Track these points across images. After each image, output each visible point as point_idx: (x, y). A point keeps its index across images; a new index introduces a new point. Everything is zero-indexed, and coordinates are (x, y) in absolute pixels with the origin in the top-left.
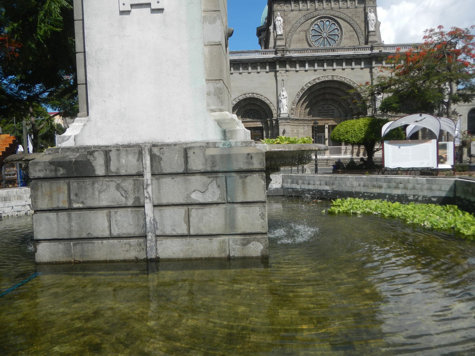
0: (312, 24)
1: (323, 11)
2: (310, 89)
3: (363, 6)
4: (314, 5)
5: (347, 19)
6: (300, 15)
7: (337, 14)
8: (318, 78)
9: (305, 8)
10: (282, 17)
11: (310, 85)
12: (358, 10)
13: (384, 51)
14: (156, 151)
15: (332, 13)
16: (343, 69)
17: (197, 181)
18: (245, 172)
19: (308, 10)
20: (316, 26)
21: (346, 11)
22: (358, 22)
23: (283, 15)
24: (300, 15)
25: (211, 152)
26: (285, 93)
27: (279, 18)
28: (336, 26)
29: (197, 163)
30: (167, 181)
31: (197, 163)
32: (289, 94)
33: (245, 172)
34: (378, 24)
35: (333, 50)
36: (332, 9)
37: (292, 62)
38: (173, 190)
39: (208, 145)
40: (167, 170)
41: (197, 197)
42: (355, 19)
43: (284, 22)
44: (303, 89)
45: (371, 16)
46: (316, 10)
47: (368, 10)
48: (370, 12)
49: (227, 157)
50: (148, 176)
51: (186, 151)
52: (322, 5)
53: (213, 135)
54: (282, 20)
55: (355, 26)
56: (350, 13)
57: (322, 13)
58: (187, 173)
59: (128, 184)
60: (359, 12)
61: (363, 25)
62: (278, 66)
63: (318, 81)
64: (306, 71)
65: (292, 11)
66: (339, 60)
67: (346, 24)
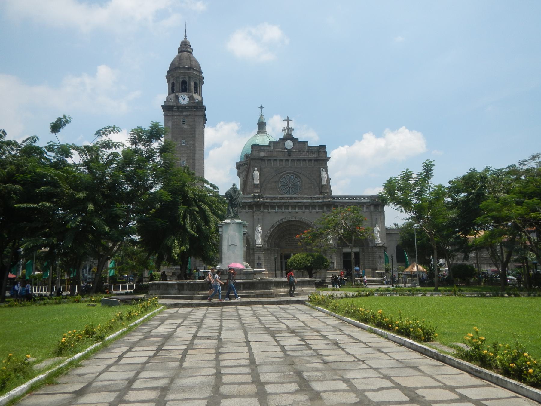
0: (281, 177)
2: (278, 226)
8: (285, 218)
11: (278, 223)
13: (331, 200)
16: (304, 212)
18: (250, 274)
26: (260, 229)
32: (263, 229)
33: (250, 274)
34: (328, 180)
35: (296, 198)
37: (266, 206)
44: (273, 226)
45: (324, 174)
54: (258, 173)
58: (240, 274)
62: (254, 208)
63: (284, 220)
64: (276, 212)
66: (300, 206)
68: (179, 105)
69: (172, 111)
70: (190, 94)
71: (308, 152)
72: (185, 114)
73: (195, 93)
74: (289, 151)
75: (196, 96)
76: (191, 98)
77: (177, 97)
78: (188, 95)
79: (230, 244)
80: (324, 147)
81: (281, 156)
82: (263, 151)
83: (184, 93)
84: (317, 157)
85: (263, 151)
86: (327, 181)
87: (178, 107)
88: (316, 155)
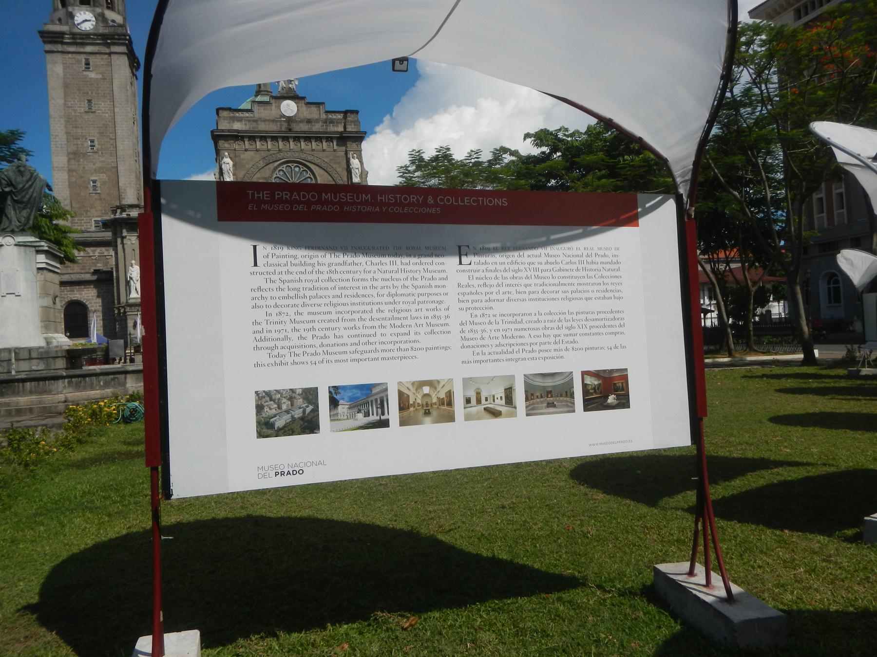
1: (290, 154)
3: (344, 148)
4: (276, 144)
5: (323, 165)
6: (258, 157)
7: (310, 158)
9: (265, 147)
10: (231, 159)
12: (339, 154)
14: (17, 351)
15: (303, 156)
17: (34, 362)
19: (268, 150)
20: (281, 173)
21: (321, 154)
22: (338, 170)
23: (232, 155)
24: (258, 157)
25: (41, 350)
27: (227, 160)
28: (309, 174)
29: (34, 355)
30: (22, 362)
31: (34, 355)
36: (302, 150)
38: (24, 366)
39: (40, 348)
40: (22, 357)
41: (34, 368)
42: (334, 166)
43: (234, 165)
45: (355, 163)
46: (280, 151)
47: (350, 154)
48: (353, 158)
49: (47, 352)
50: (13, 360)
51: (30, 350)
52: (287, 144)
53: (43, 344)
54: (231, 163)
55: (334, 175)
56: (327, 157)
57: (289, 156)
58: (30, 359)
59: (5, 364)
60: (338, 157)
61: (345, 174)
65: (246, 150)
67: (322, 171)
68: (76, 30)
69: (63, 43)
70: (99, 10)
71: (326, 122)
72: (89, 49)
73: (108, 8)
74: (290, 120)
75: (110, 15)
76: (101, 18)
77: (71, 16)
78: (93, 12)
79: (4, 292)
80: (357, 112)
81: (274, 127)
82: (240, 120)
83: (84, 7)
84: (341, 133)
85: (238, 121)
86: (361, 176)
87: (74, 35)
88: (340, 129)
